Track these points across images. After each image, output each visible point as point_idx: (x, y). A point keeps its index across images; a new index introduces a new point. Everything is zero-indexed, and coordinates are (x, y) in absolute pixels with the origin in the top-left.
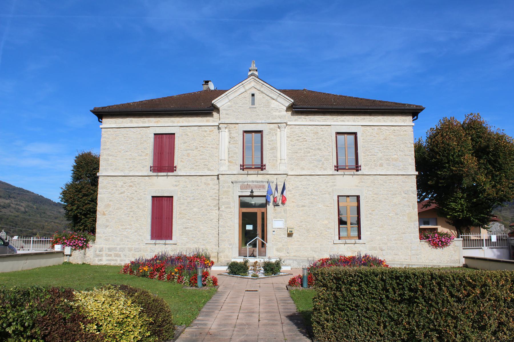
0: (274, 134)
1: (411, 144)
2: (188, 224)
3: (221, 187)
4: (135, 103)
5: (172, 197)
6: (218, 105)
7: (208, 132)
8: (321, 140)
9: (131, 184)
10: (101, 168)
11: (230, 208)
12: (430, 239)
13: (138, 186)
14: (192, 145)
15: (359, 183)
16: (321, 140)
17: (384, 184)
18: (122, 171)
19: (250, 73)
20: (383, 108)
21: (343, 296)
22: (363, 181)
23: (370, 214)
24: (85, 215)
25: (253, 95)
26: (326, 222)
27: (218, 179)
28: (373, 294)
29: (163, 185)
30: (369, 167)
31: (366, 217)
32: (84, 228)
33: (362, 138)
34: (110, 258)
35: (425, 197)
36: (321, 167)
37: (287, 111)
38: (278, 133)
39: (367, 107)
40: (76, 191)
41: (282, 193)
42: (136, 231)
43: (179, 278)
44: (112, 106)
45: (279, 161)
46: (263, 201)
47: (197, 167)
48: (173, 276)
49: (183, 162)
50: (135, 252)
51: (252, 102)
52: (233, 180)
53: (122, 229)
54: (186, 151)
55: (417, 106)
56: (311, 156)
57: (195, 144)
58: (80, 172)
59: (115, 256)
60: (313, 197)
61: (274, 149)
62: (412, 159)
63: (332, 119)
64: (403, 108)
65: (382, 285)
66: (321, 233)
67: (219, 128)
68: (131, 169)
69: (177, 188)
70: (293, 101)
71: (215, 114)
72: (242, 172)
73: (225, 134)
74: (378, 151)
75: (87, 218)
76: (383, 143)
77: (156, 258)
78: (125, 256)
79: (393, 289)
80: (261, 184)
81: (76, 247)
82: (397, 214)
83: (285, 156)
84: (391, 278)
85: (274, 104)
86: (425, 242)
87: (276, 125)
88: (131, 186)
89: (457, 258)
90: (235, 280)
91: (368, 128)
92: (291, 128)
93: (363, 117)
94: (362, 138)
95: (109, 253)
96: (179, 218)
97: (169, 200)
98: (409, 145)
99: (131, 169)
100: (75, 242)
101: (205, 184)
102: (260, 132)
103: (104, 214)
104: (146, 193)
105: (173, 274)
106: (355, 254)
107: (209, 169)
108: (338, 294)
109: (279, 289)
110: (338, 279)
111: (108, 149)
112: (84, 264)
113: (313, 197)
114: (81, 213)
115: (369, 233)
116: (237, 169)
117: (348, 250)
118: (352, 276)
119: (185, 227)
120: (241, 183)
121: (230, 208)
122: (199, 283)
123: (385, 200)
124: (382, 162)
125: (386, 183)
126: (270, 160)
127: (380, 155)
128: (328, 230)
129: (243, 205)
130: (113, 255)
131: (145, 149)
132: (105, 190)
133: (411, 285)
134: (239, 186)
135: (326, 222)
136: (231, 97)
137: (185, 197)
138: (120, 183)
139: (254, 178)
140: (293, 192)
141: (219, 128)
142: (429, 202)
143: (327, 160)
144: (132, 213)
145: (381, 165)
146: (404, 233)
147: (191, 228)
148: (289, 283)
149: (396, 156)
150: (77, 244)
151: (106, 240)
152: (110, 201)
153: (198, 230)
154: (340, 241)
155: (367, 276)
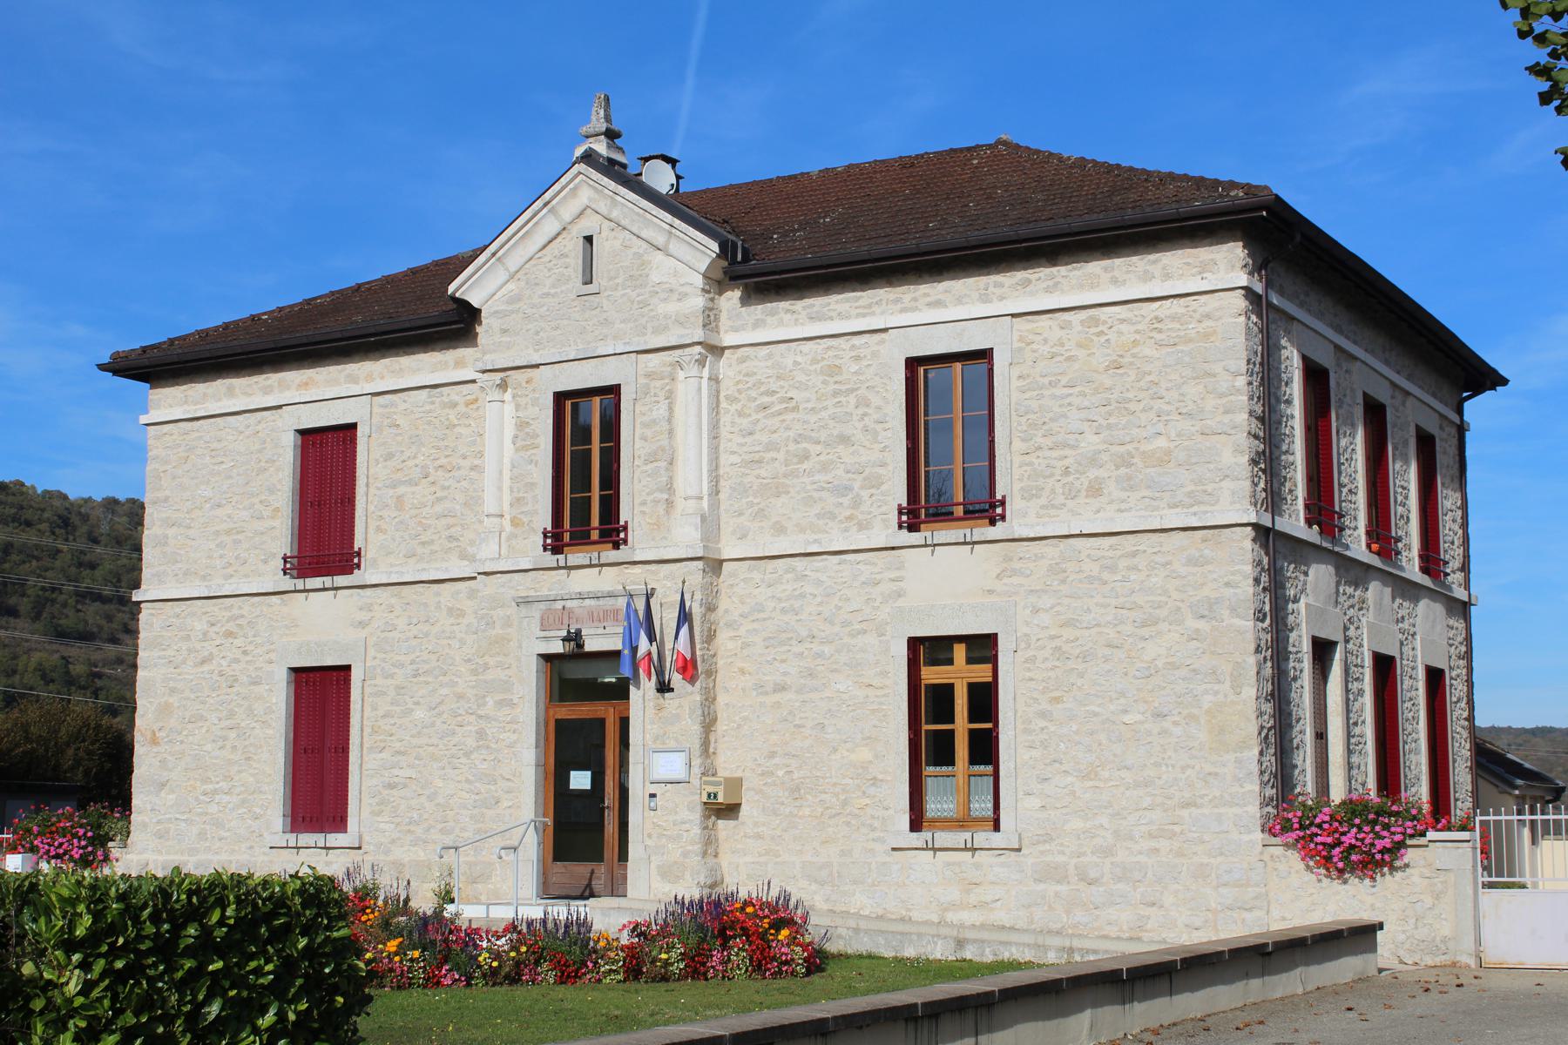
0: (662, 394)
2: (396, 771)
5: (348, 668)
7: (461, 408)
8: (852, 399)
9: (231, 626)
10: (146, 574)
11: (511, 704)
14: (410, 463)
16: (852, 399)
17: (1106, 575)
22: (1017, 565)
23: (1043, 715)
30: (1043, 501)
31: (1026, 731)
36: (849, 518)
44: (183, 338)
49: (384, 532)
54: (394, 487)
60: (816, 647)
62: (1237, 451)
63: (897, 301)
66: (845, 803)
68: (230, 571)
72: (550, 559)
82: (1159, 716)
85: (661, 269)
86: (1287, 845)
88: (229, 634)
89: (1446, 930)
92: (742, 360)
93: (1020, 275)
99: (230, 571)
103: (154, 741)
104: (273, 656)
111: (166, 499)
113: (816, 647)
115: (1035, 802)
116: (532, 549)
120: (542, 606)
121: (511, 704)
123: (1108, 651)
124: (1102, 473)
125: (1112, 569)
127: (1091, 442)
128: (872, 791)
131: (272, 491)
132: (156, 653)
134: (538, 615)
135: (865, 754)
136: (513, 262)
138: (199, 626)
144: (233, 734)
145: (1095, 490)
146: (1187, 805)
147: (405, 786)
149: (1162, 442)
151: (160, 836)
152: (173, 691)
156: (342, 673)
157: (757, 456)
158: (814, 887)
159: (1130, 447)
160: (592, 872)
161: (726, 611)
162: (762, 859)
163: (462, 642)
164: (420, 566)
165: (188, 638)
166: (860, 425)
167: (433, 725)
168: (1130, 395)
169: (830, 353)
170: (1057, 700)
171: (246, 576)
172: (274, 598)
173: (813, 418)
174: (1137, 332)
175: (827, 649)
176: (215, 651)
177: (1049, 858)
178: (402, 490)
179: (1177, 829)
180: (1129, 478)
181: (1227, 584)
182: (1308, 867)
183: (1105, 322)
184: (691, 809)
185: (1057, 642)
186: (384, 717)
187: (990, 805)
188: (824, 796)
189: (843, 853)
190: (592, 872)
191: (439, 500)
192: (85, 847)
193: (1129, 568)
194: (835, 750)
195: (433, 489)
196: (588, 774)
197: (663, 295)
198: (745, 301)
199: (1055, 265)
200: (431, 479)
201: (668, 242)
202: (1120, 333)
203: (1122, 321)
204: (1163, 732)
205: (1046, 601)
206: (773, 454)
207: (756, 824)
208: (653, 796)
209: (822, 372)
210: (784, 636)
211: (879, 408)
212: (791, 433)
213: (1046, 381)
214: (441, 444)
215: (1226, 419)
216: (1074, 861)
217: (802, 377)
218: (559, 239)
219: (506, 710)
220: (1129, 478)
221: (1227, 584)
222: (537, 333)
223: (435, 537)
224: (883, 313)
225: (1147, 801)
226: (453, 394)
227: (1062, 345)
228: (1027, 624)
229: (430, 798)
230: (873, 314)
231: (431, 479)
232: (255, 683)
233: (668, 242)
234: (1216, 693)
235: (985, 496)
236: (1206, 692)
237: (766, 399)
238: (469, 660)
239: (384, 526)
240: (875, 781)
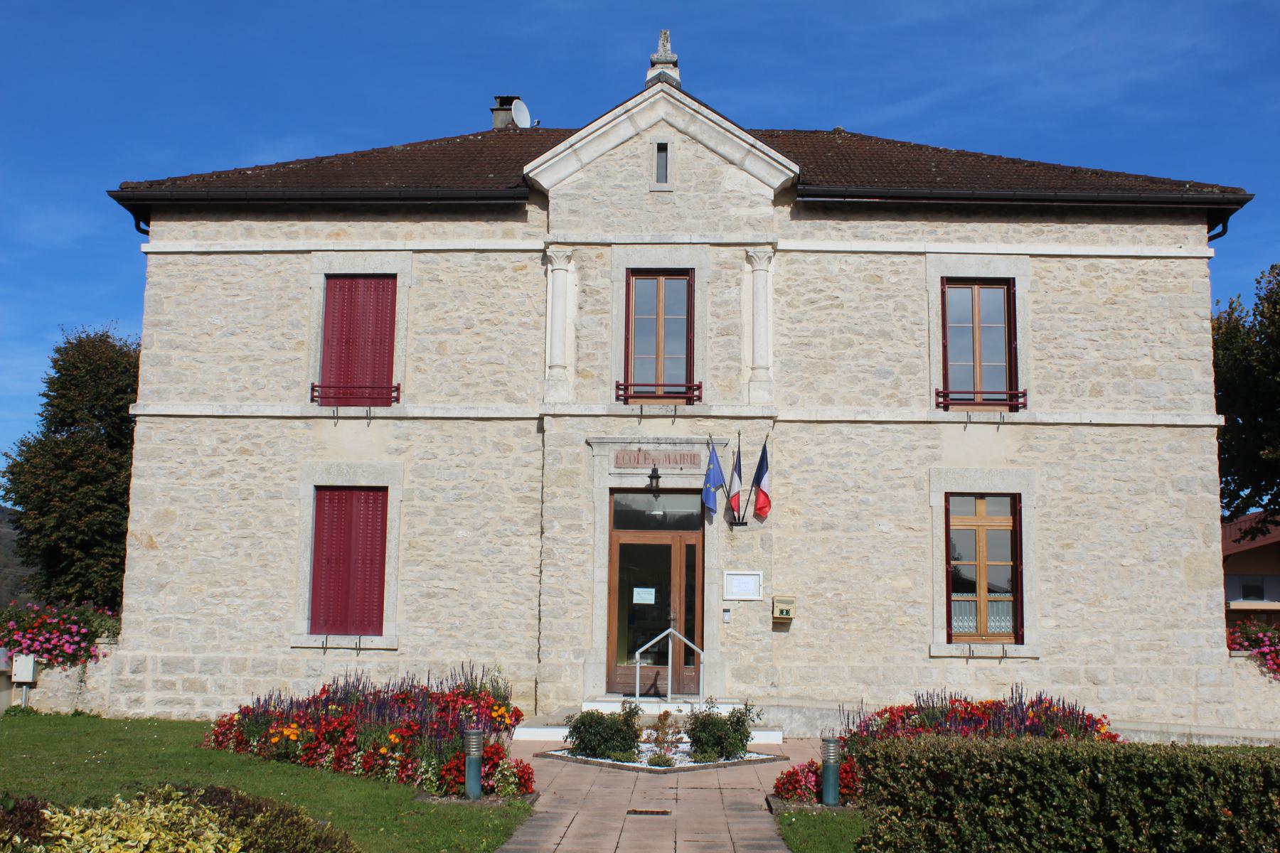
0: (733, 282)
1: (1203, 318)
2: (436, 583)
3: (549, 460)
4: (262, 168)
5: (385, 489)
6: (545, 181)
7: (509, 273)
9: (246, 444)
10: (142, 388)
11: (579, 528)
12: (1266, 649)
13: (269, 452)
14: (454, 314)
15: (1019, 450)
17: (1106, 455)
18: (215, 398)
19: (652, 73)
20: (1105, 194)
21: (958, 836)
22: (1034, 443)
23: (1057, 557)
24: (86, 547)
25: (662, 148)
26: (905, 582)
27: (541, 430)
28: (1062, 833)
29: (355, 447)
30: (1055, 396)
31: (1043, 568)
32: (80, 591)
33: (1033, 297)
34: (168, 695)
35: (1249, 502)
36: (891, 396)
37: (776, 202)
38: (747, 278)
39: (1050, 193)
40: (57, 467)
41: (757, 480)
42: (259, 605)
43: (403, 766)
44: (184, 179)
45: (747, 373)
46: (690, 506)
47: (472, 391)
48: (384, 757)
49: (425, 372)
50: (256, 674)
51: (656, 173)
52: (592, 435)
53: (213, 596)
54: (434, 333)
55: (1224, 190)
56: (855, 357)
57: (463, 312)
58: (71, 400)
59: (185, 689)
60: (861, 496)
61: (730, 331)
62: (1205, 373)
63: (931, 233)
64: (1175, 195)
65: (1092, 803)
66: (888, 620)
67: (546, 260)
68: (246, 394)
69: (400, 459)
70: (796, 169)
71: (532, 210)
72: (621, 408)
73: (565, 279)
74: (1088, 344)
75: (92, 556)
76: (1106, 314)
77: (328, 696)
78: (222, 687)
79: (1132, 817)
80: (686, 449)
81: (51, 656)
83: (766, 356)
84: (1126, 781)
85: (733, 179)
86: (1249, 657)
87: (739, 251)
88: (243, 451)
90: (593, 776)
91: (1054, 263)
92: (792, 262)
93: (1035, 226)
94: (1033, 297)
95: (167, 678)
96: (407, 562)
97: (375, 500)
98: (1196, 324)
99: (246, 394)
100: (48, 640)
101: (497, 446)
102: (687, 273)
103: (151, 545)
105: (383, 750)
106: (1002, 695)
107: (510, 399)
108: (942, 828)
109: (741, 808)
110: (942, 779)
111: (169, 323)
112: (77, 713)
113: (861, 496)
114: (70, 541)
115: (1051, 623)
116: (604, 399)
117: (978, 679)
118: (991, 771)
119: (425, 590)
120: (617, 447)
121: (579, 528)
122: (472, 785)
123: (1108, 512)
124: (1100, 379)
125: (1111, 451)
126: (717, 368)
127: (1093, 356)
128: (911, 611)
129: (623, 518)
130: (179, 686)
131: (295, 325)
132: (155, 464)
133: (1192, 805)
134: (612, 455)
135: (905, 582)
136: (586, 156)
137: (427, 490)
138: (208, 442)
139: (661, 428)
140: (793, 479)
141: (546, 260)
142: (1264, 521)
143: (911, 370)
144: (246, 543)
145: (1097, 391)
146: (1173, 626)
147: (446, 596)
148: (776, 787)
149: (1147, 361)
150: (55, 647)
151: (156, 633)
152: (174, 500)
153: (470, 602)
154: (953, 649)
155: (1041, 770)
157: (806, 341)
158: (861, 686)
159: (1125, 363)
160: (658, 674)
161: (778, 462)
162: (812, 664)
163: (508, 472)
164: (465, 404)
165: (194, 452)
166: (899, 325)
168: (1123, 325)
169: (871, 265)
170: (1069, 546)
171: (265, 400)
172: (297, 422)
173: (857, 315)
174: (1128, 279)
175: (871, 498)
176: (227, 466)
177: (1063, 665)
178: (443, 337)
179: (1164, 644)
180: (1124, 386)
182: (1262, 672)
183: (1102, 270)
184: (761, 621)
185: (1069, 503)
186: (421, 534)
187: (954, 624)
188: (868, 615)
189: (886, 659)
190: (658, 674)
191: (483, 349)
192: (78, 643)
193: (1124, 451)
194: (879, 578)
195: (478, 339)
196: (653, 591)
197: (734, 201)
198: (796, 215)
199: (1063, 222)
200: (476, 330)
202: (1114, 278)
204: (1151, 573)
206: (822, 340)
207: (806, 636)
208: (725, 611)
209: (865, 280)
210: (833, 485)
211: (915, 313)
212: (836, 325)
213: (1056, 307)
214: (487, 301)
215: (1197, 349)
216: (1083, 667)
217: (845, 281)
218: (630, 142)
219: (574, 534)
220: (1124, 386)
221: (1201, 468)
222: (608, 217)
223: (480, 380)
224: (920, 240)
225: (1141, 623)
226: (500, 259)
227: (1069, 282)
229: (473, 608)
230: (911, 239)
231: (476, 330)
232: (272, 498)
234: (1193, 546)
236: (1185, 544)
237: (813, 296)
238: (517, 489)
239: (423, 366)
240: (914, 603)
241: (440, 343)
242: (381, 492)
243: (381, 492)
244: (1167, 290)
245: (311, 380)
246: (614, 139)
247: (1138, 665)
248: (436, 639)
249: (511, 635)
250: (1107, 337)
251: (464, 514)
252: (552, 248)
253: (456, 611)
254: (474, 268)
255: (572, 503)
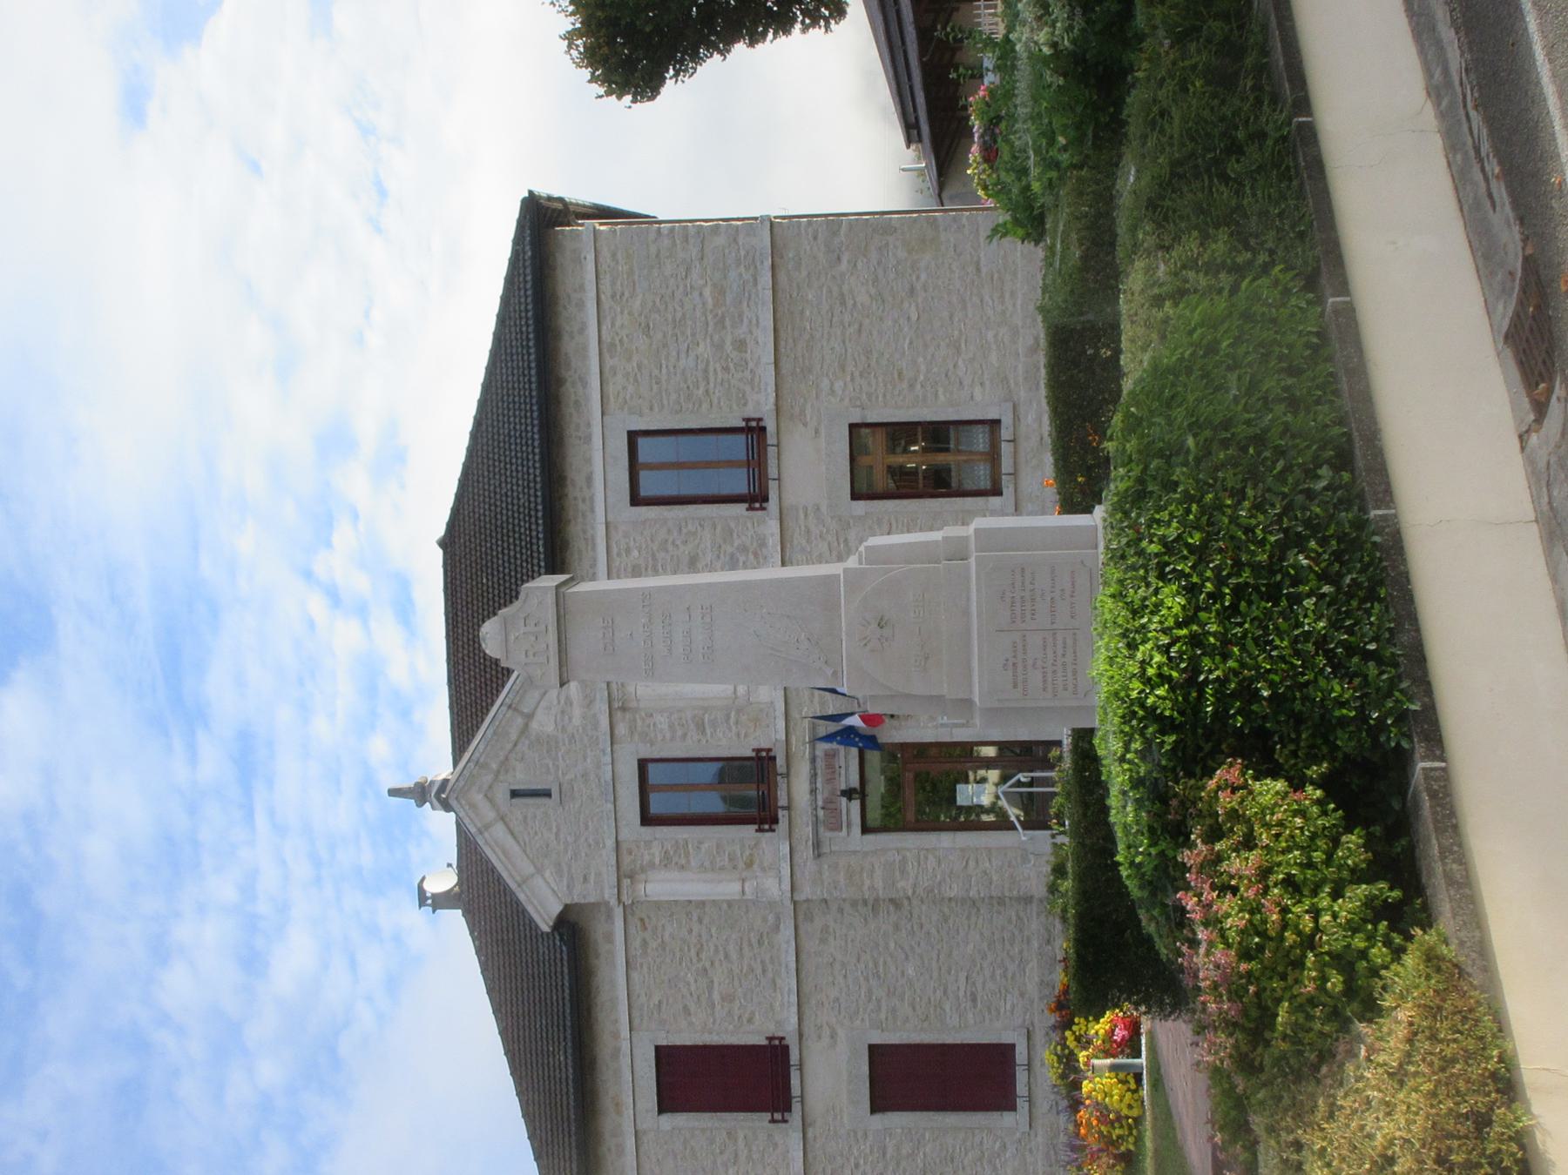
6: (556, 909)
11: (904, 860)
14: (693, 988)
15: (805, 425)
22: (797, 409)
23: (912, 386)
25: (515, 794)
29: (831, 1077)
30: (748, 388)
46: (874, 757)
47: (770, 967)
49: (753, 1013)
57: (690, 977)
69: (841, 1033)
74: (692, 355)
76: (659, 336)
80: (820, 764)
82: (912, 291)
85: (544, 723)
91: (611, 390)
101: (823, 941)
102: (643, 765)
107: (776, 928)
115: (977, 391)
116: (773, 845)
119: (969, 1004)
120: (821, 829)
127: (704, 349)
129: (893, 821)
134: (829, 834)
137: (871, 1006)
145: (741, 345)
146: (978, 270)
149: (707, 292)
154: (1008, 490)
156: (879, 1055)
167: (921, 957)
170: (900, 374)
172: (810, 1134)
177: (1021, 379)
178: (716, 996)
181: (815, 238)
185: (857, 374)
191: (727, 956)
200: (708, 965)
201: (522, 713)
203: (613, 325)
205: (825, 383)
211: (669, 531)
215: (692, 241)
221: (815, 238)
225: (976, 299)
228: (842, 400)
229: (984, 957)
231: (708, 965)
232: (884, 1154)
233: (522, 713)
235: (741, 439)
241: (723, 999)
242: (874, 1050)
243: (874, 1050)
244: (631, 272)
245: (766, 1124)
246: (510, 842)
247: (1019, 302)
248: (1016, 993)
249: (1010, 921)
250: (683, 333)
251: (893, 969)
252: (624, 898)
253: (987, 973)
254: (645, 969)
255: (878, 873)
